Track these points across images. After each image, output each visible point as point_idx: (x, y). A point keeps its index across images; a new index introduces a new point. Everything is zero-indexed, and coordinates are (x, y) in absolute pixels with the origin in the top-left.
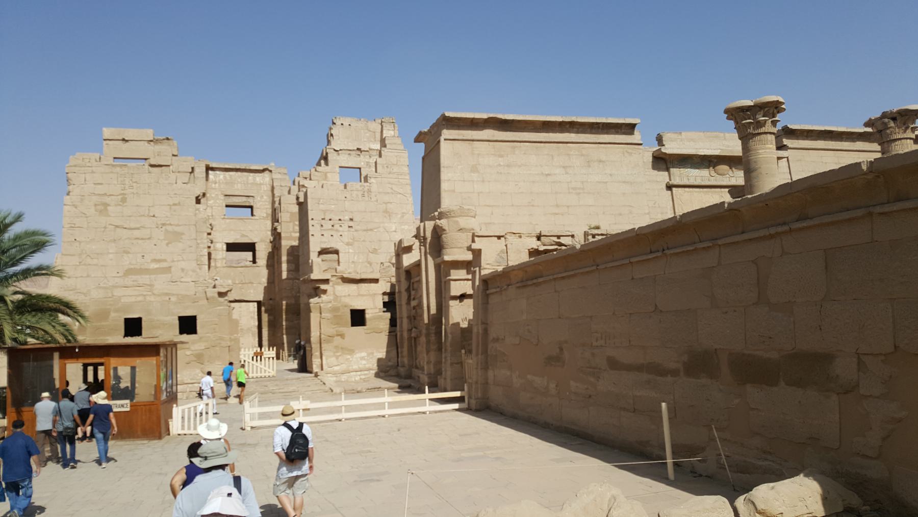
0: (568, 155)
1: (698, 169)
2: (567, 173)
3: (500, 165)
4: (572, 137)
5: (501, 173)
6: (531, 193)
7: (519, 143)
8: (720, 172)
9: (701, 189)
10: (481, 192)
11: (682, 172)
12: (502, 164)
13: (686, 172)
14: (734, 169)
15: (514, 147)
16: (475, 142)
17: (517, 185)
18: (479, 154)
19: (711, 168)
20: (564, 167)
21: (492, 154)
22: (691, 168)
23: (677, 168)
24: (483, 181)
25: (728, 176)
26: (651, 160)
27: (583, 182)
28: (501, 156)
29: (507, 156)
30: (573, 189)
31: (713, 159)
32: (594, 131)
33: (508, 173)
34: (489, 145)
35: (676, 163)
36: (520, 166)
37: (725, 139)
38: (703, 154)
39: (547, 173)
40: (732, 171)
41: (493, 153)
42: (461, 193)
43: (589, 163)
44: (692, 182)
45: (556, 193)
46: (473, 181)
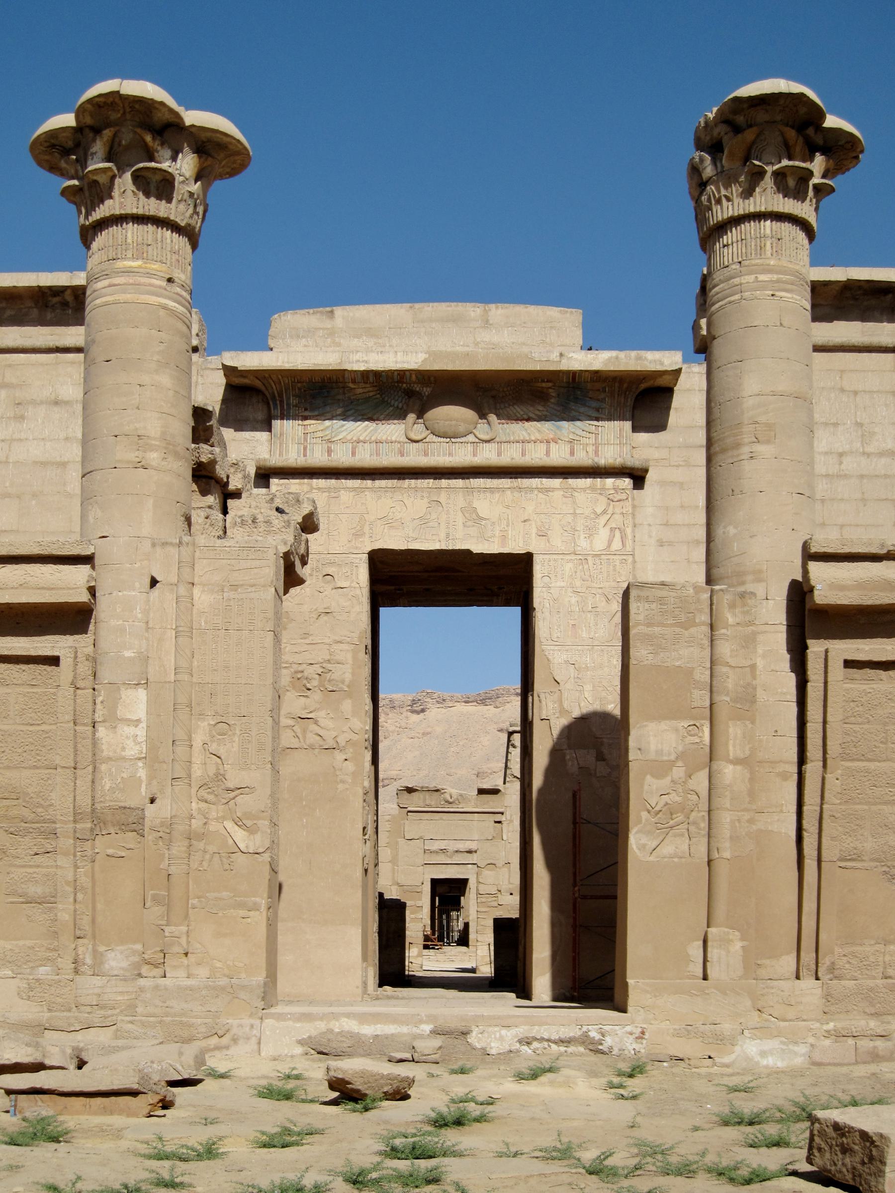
1: (370, 419)
8: (442, 426)
9: (369, 483)
11: (310, 429)
13: (328, 427)
14: (492, 417)
19: (411, 417)
22: (345, 417)
23: (295, 418)
25: (471, 438)
26: (220, 397)
31: (417, 388)
32: (49, 316)
35: (294, 401)
38: (362, 367)
40: (489, 423)
44: (342, 458)
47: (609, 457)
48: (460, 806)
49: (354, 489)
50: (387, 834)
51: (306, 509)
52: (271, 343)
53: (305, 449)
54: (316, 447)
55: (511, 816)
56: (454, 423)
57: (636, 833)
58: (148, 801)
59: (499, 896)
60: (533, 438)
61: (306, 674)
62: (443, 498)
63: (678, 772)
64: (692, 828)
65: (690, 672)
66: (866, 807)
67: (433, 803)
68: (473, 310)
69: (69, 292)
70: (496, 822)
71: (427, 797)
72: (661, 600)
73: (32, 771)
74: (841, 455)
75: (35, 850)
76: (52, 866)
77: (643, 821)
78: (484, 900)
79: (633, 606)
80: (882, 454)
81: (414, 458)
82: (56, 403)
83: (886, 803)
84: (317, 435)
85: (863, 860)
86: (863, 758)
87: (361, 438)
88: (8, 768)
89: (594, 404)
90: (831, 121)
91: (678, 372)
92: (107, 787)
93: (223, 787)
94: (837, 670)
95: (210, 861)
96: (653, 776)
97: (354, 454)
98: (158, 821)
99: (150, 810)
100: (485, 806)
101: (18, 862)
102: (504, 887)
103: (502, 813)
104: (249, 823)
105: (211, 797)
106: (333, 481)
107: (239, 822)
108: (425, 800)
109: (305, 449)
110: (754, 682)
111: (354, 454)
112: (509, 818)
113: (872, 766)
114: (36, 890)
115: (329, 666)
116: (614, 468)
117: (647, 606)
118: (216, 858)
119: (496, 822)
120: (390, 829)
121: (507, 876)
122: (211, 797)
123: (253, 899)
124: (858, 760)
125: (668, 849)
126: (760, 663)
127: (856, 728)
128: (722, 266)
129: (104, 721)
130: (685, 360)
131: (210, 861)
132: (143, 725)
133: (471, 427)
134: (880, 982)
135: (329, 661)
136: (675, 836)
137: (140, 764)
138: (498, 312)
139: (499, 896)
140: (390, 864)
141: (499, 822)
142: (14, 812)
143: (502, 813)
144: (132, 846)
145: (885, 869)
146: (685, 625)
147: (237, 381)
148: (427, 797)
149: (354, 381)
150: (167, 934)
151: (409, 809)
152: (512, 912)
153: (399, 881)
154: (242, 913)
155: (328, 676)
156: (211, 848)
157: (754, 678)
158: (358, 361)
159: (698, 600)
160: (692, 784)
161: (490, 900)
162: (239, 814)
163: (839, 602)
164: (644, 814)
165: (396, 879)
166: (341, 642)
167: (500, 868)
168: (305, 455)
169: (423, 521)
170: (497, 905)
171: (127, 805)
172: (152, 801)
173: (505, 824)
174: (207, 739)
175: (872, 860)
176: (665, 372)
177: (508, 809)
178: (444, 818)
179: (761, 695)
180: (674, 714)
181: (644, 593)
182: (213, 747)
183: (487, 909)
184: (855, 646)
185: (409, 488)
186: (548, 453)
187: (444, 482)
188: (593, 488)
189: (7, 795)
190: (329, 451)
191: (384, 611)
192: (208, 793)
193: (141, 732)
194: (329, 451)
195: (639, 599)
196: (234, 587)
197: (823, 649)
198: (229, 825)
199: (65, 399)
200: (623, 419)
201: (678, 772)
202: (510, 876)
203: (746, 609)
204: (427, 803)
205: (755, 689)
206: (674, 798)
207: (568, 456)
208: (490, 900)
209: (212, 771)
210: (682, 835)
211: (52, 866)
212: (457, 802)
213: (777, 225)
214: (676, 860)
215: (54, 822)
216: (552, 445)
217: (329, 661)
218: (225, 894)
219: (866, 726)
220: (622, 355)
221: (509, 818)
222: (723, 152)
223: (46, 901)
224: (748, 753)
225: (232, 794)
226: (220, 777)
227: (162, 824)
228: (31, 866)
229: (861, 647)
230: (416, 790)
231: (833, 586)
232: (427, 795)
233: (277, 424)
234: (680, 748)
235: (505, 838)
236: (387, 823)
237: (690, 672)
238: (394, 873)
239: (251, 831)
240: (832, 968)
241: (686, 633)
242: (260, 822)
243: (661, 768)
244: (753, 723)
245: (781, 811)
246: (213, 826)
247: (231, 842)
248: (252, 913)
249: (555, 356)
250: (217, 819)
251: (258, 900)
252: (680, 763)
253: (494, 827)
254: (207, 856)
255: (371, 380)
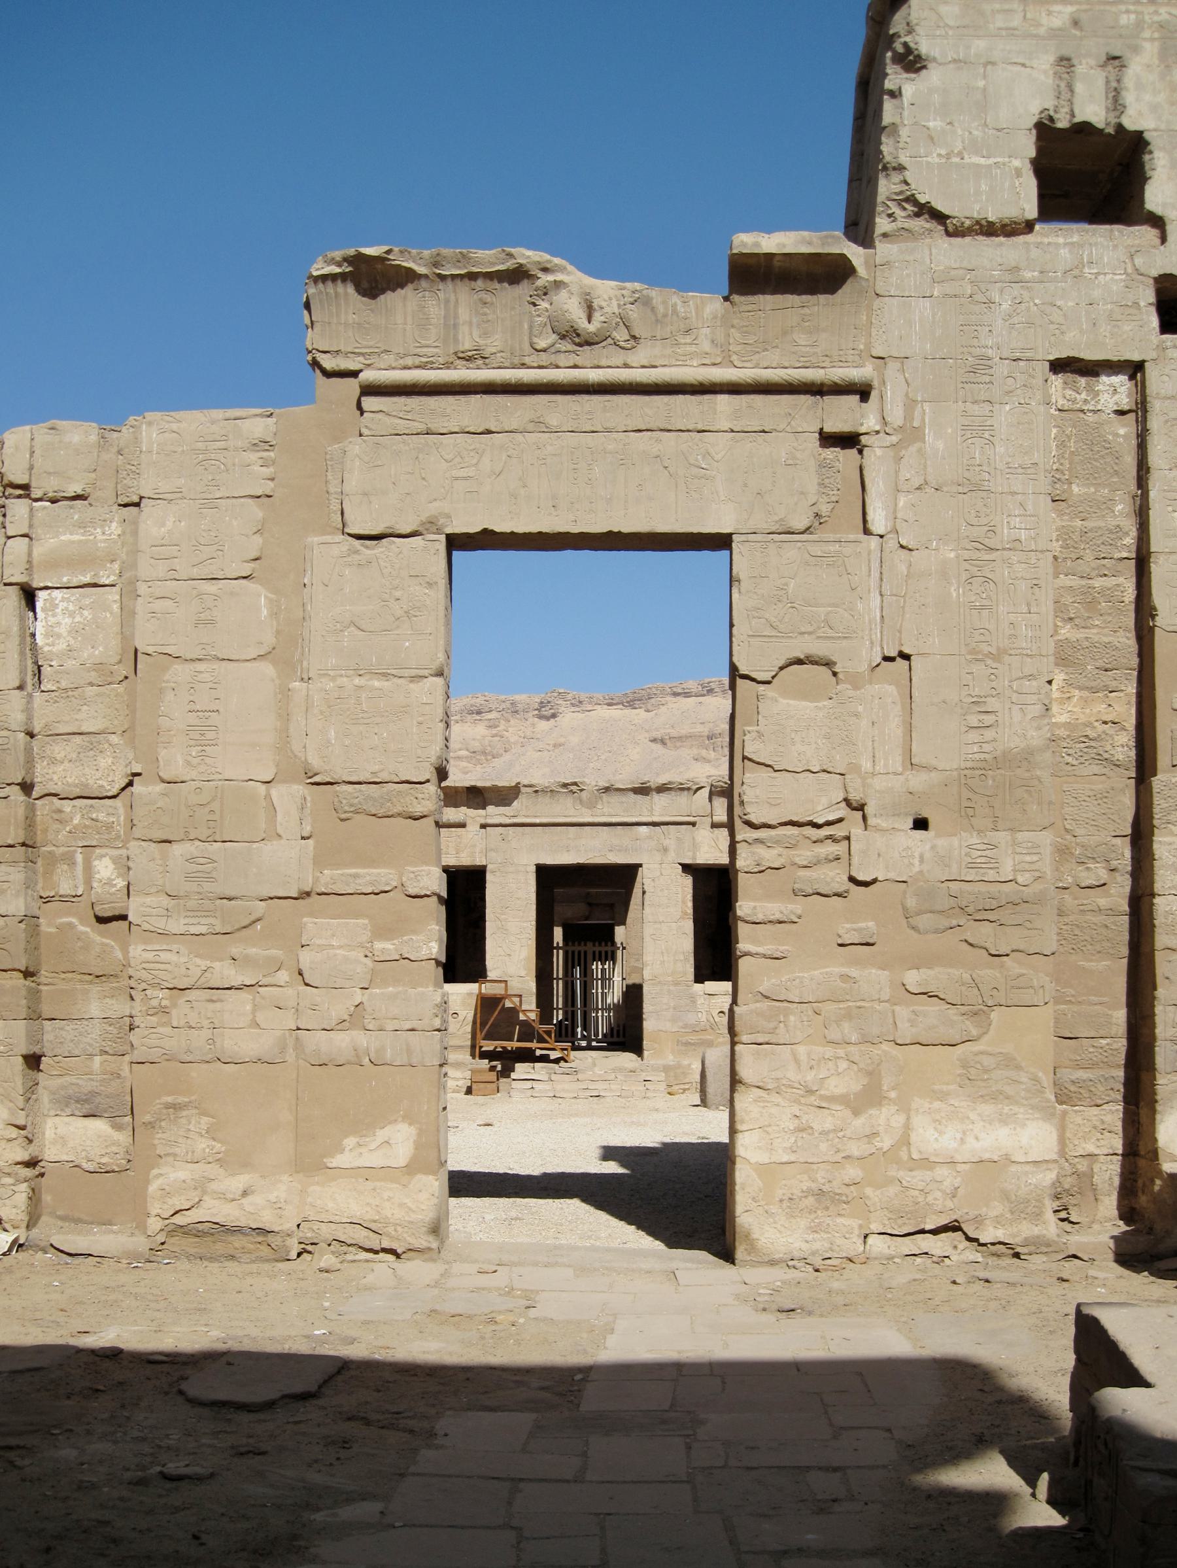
48: (640, 355)
50: (256, 511)
55: (910, 404)
59: (857, 831)
67: (493, 344)
70: (830, 440)
71: (464, 313)
78: (770, 856)
100: (773, 357)
102: (878, 783)
103: (863, 392)
108: (451, 326)
112: (896, 416)
119: (830, 440)
120: (268, 487)
121: (894, 727)
139: (857, 831)
140: (268, 669)
141: (849, 441)
143: (863, 392)
148: (464, 313)
151: (368, 376)
152: (924, 921)
153: (315, 762)
161: (805, 854)
165: (296, 746)
167: (856, 682)
170: (842, 884)
173: (876, 455)
177: (892, 366)
178: (553, 421)
183: (795, 907)
202: (909, 729)
204: (466, 344)
208: (805, 854)
212: (621, 335)
221: (896, 416)
230: (403, 278)
232: (464, 299)
235: (878, 520)
236: (253, 457)
238: (285, 717)
253: (823, 465)
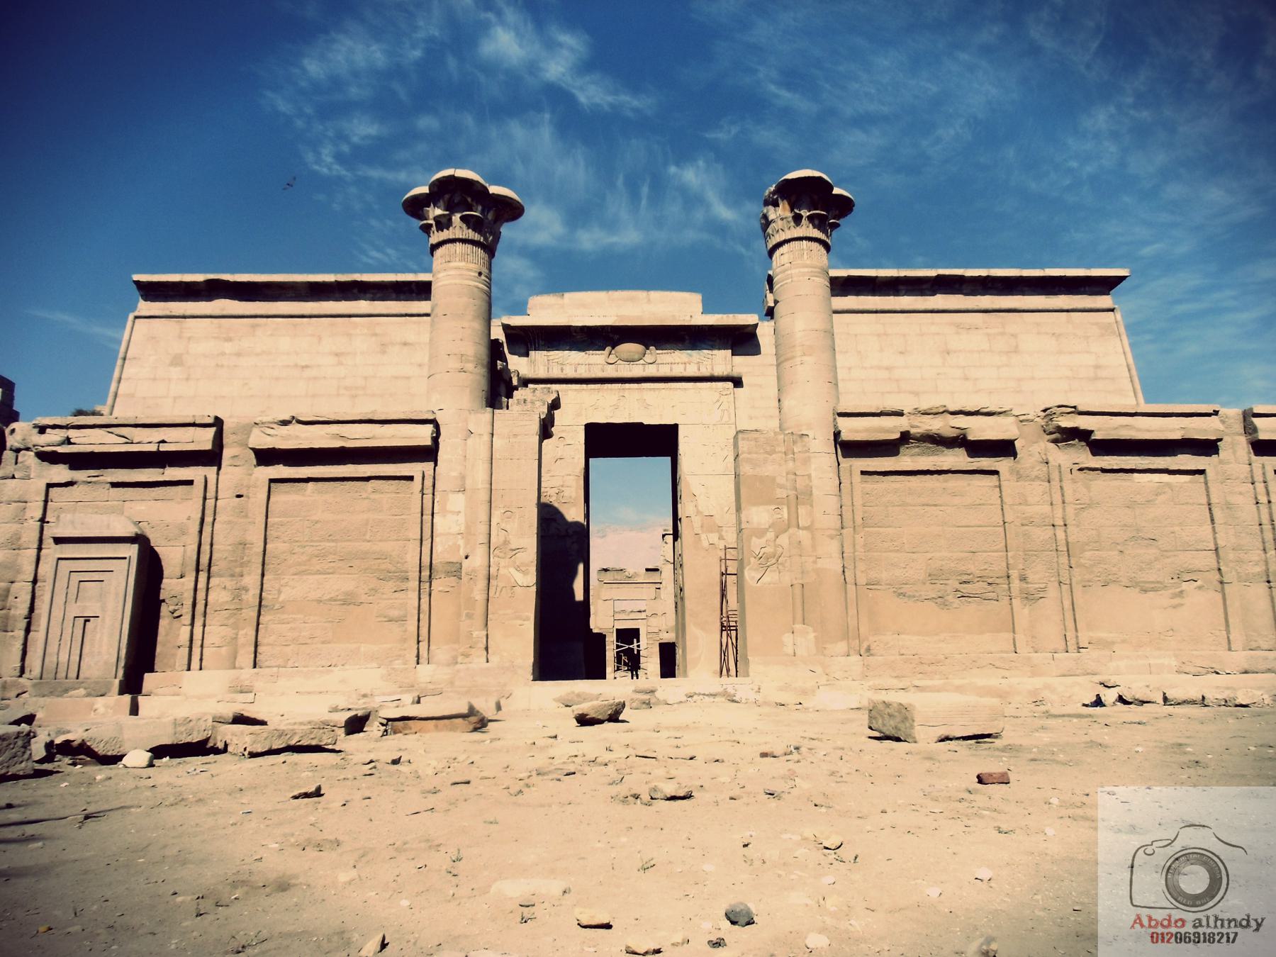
0: (349, 335)
2: (340, 364)
3: (223, 354)
4: (363, 306)
5: (222, 366)
6: (269, 396)
7: (265, 319)
10: (180, 397)
12: (227, 352)
15: (254, 326)
16: (187, 320)
17: (246, 384)
18: (189, 338)
19: (608, 349)
20: (337, 355)
21: (215, 338)
24: (187, 379)
25: (642, 362)
27: (366, 378)
28: (229, 339)
29: (240, 340)
30: (346, 388)
31: (611, 335)
33: (235, 366)
34: (212, 323)
36: (257, 355)
37: (649, 301)
38: (580, 324)
39: (304, 364)
41: (216, 335)
42: (144, 398)
43: (384, 348)
45: (314, 396)
46: (170, 380)
47: (718, 371)
49: (576, 390)
51: (554, 396)
52: (528, 312)
53: (548, 369)
54: (554, 368)
56: (632, 354)
57: (749, 570)
58: (464, 557)
60: (677, 361)
61: (548, 494)
62: (626, 394)
63: (771, 535)
64: (780, 567)
65: (774, 479)
66: (879, 554)
68: (641, 294)
69: (414, 284)
72: (756, 440)
73: (395, 542)
74: (850, 369)
75: (395, 589)
76: (404, 599)
77: (752, 563)
79: (740, 443)
80: (872, 368)
81: (610, 372)
82: (405, 344)
83: (891, 551)
84: (555, 360)
85: (881, 585)
86: (876, 526)
87: (580, 362)
88: (380, 541)
89: (710, 343)
90: (836, 191)
91: (756, 326)
92: (439, 551)
93: (509, 548)
94: (857, 477)
95: (501, 592)
96: (756, 537)
97: (576, 371)
98: (470, 569)
99: (466, 563)
101: (385, 596)
104: (523, 569)
105: (501, 555)
106: (564, 385)
107: (518, 569)
109: (548, 369)
110: (810, 484)
111: (576, 371)
113: (881, 530)
114: (395, 613)
115: (563, 489)
116: (722, 377)
117: (748, 442)
118: (504, 589)
122: (501, 555)
123: (527, 614)
124: (873, 527)
125: (766, 579)
126: (813, 475)
127: (870, 508)
128: (778, 265)
129: (438, 513)
130: (760, 319)
131: (501, 592)
132: (462, 515)
133: (641, 356)
134: (898, 657)
135: (562, 486)
136: (771, 571)
137: (460, 537)
138: (655, 295)
142: (383, 567)
144: (453, 585)
145: (894, 589)
146: (770, 453)
147: (509, 332)
149: (575, 332)
150: (474, 636)
154: (520, 622)
155: (562, 494)
156: (501, 585)
157: (811, 481)
158: (578, 321)
159: (777, 440)
160: (778, 541)
162: (517, 564)
163: (856, 439)
164: (752, 560)
166: (570, 475)
168: (548, 371)
169: (616, 407)
171: (451, 560)
172: (467, 557)
174: (499, 521)
175: (887, 584)
176: (749, 326)
179: (815, 492)
180: (769, 502)
181: (745, 436)
182: (503, 526)
184: (866, 463)
185: (608, 389)
186: (685, 370)
187: (627, 386)
188: (711, 388)
189: (379, 556)
190: (562, 370)
191: (592, 460)
192: (500, 552)
193: (461, 518)
194: (562, 370)
195: (743, 439)
196: (515, 436)
197: (848, 465)
198: (512, 570)
199: (411, 342)
200: (725, 349)
201: (771, 535)
203: (804, 443)
205: (811, 488)
206: (769, 550)
207: (696, 371)
209: (502, 539)
210: (775, 571)
211: (404, 599)
213: (810, 244)
214: (772, 585)
215: (407, 572)
216: (687, 365)
217: (562, 486)
218: (509, 611)
219: (876, 508)
220: (725, 316)
222: (779, 206)
223: (402, 620)
224: (809, 524)
225: (514, 552)
226: (506, 542)
227: (473, 571)
228: (392, 599)
229: (870, 463)
231: (851, 431)
233: (532, 353)
234: (771, 521)
237: (774, 479)
239: (525, 573)
240: (868, 649)
241: (771, 457)
242: (530, 568)
243: (761, 533)
244: (812, 506)
245: (831, 557)
246: (502, 571)
247: (513, 580)
248: (525, 622)
249: (688, 318)
250: (505, 567)
251: (530, 614)
252: (770, 530)
254: (499, 589)
255: (586, 330)
